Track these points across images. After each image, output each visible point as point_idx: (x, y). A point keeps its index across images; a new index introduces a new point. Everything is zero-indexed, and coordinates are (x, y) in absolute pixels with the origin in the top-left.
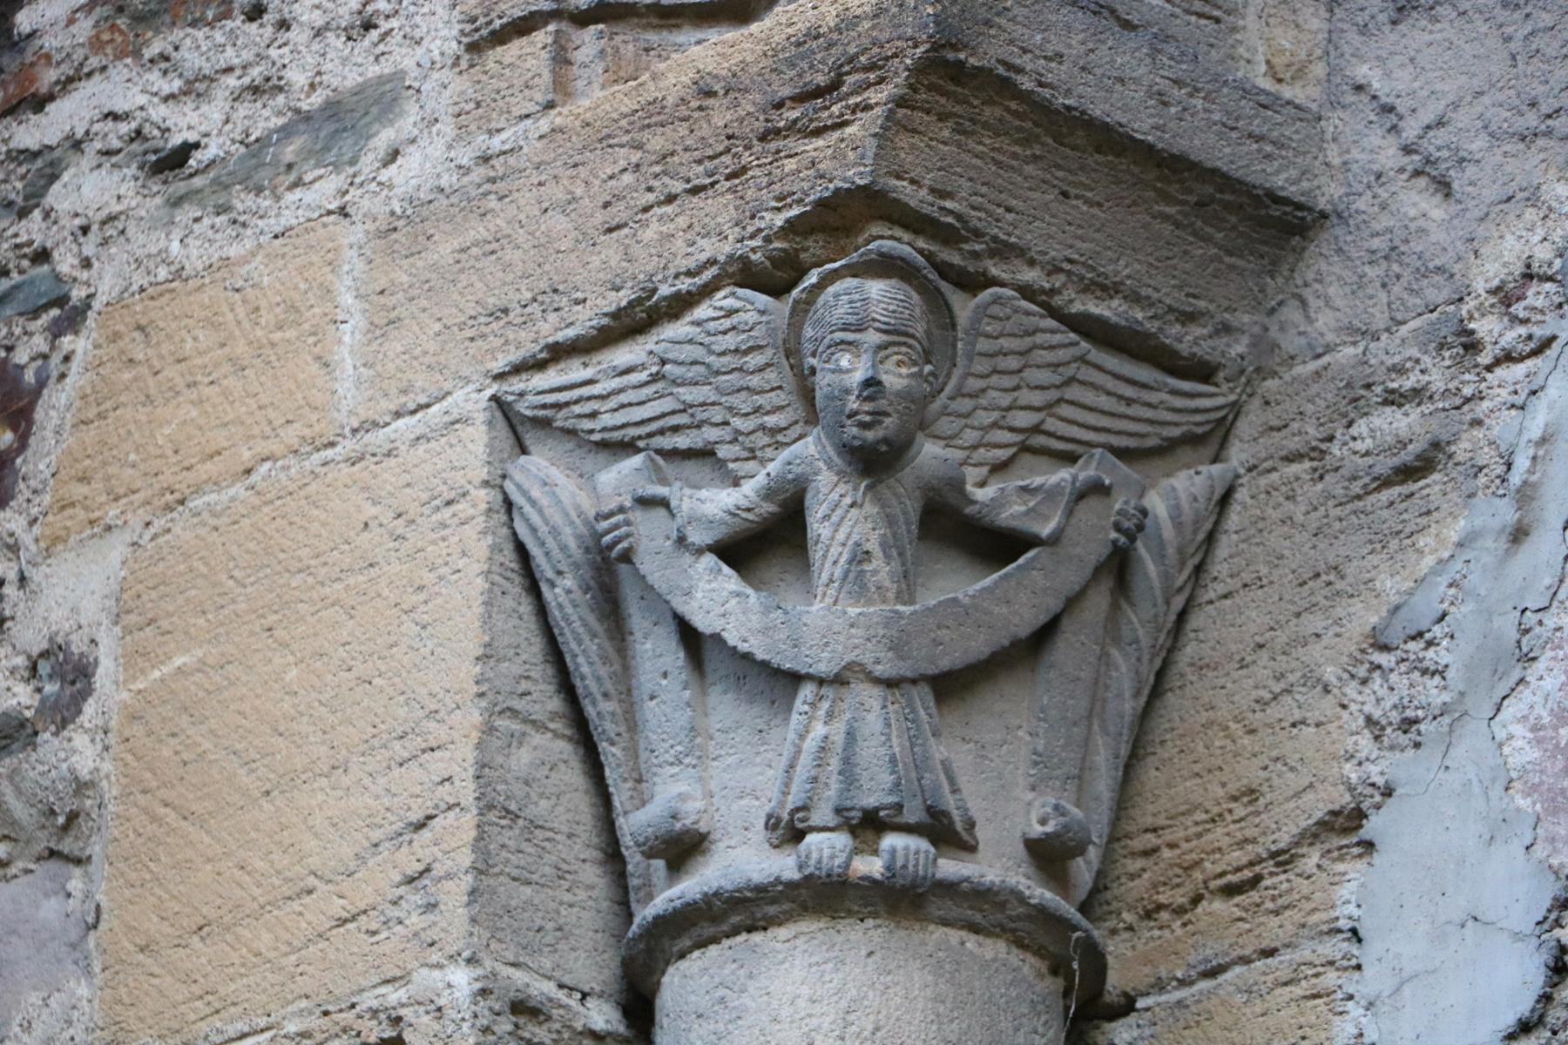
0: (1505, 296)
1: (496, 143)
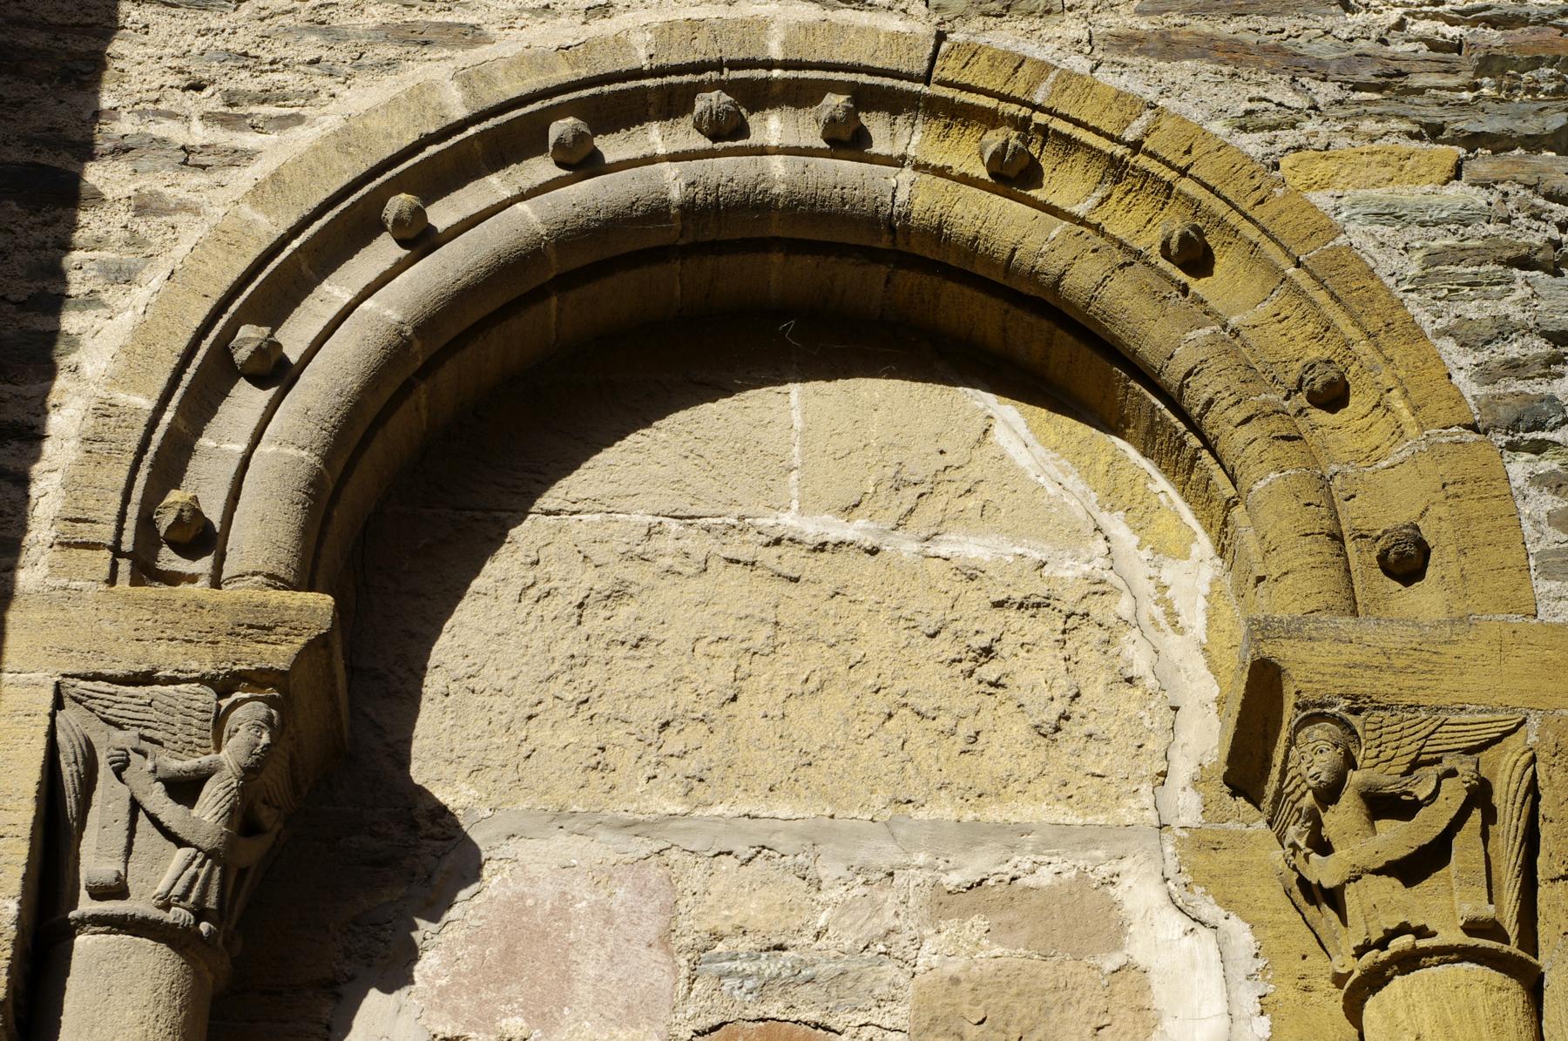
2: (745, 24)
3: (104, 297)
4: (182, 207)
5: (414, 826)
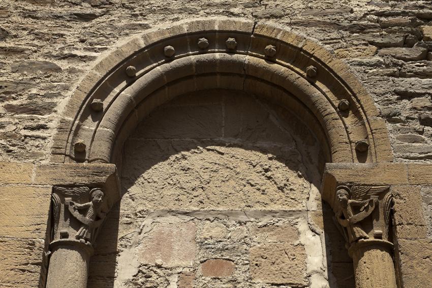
0: (140, 212)
1: (56, 163)
2: (210, 22)
3: (62, 93)
4: (80, 71)
5: (136, 215)
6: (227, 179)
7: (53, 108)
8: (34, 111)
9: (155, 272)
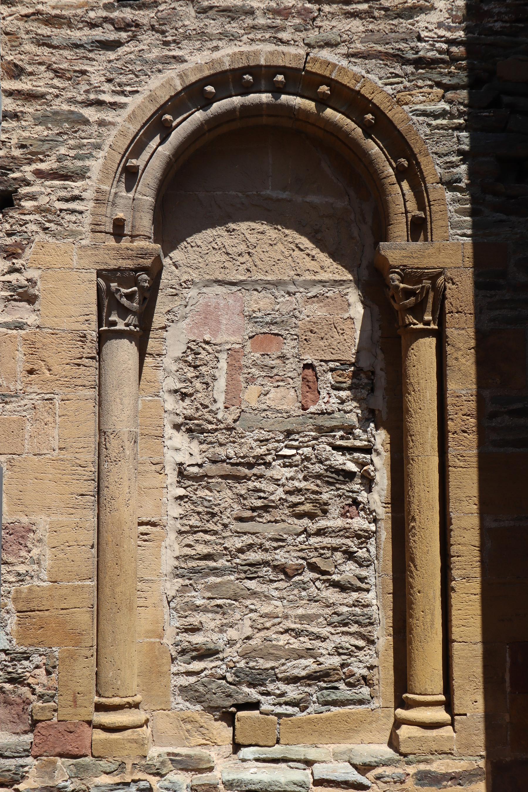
0: (185, 282)
4: (110, 123)
5: (181, 285)
6: (275, 242)
7: (86, 173)
8: (65, 177)
9: (204, 349)
